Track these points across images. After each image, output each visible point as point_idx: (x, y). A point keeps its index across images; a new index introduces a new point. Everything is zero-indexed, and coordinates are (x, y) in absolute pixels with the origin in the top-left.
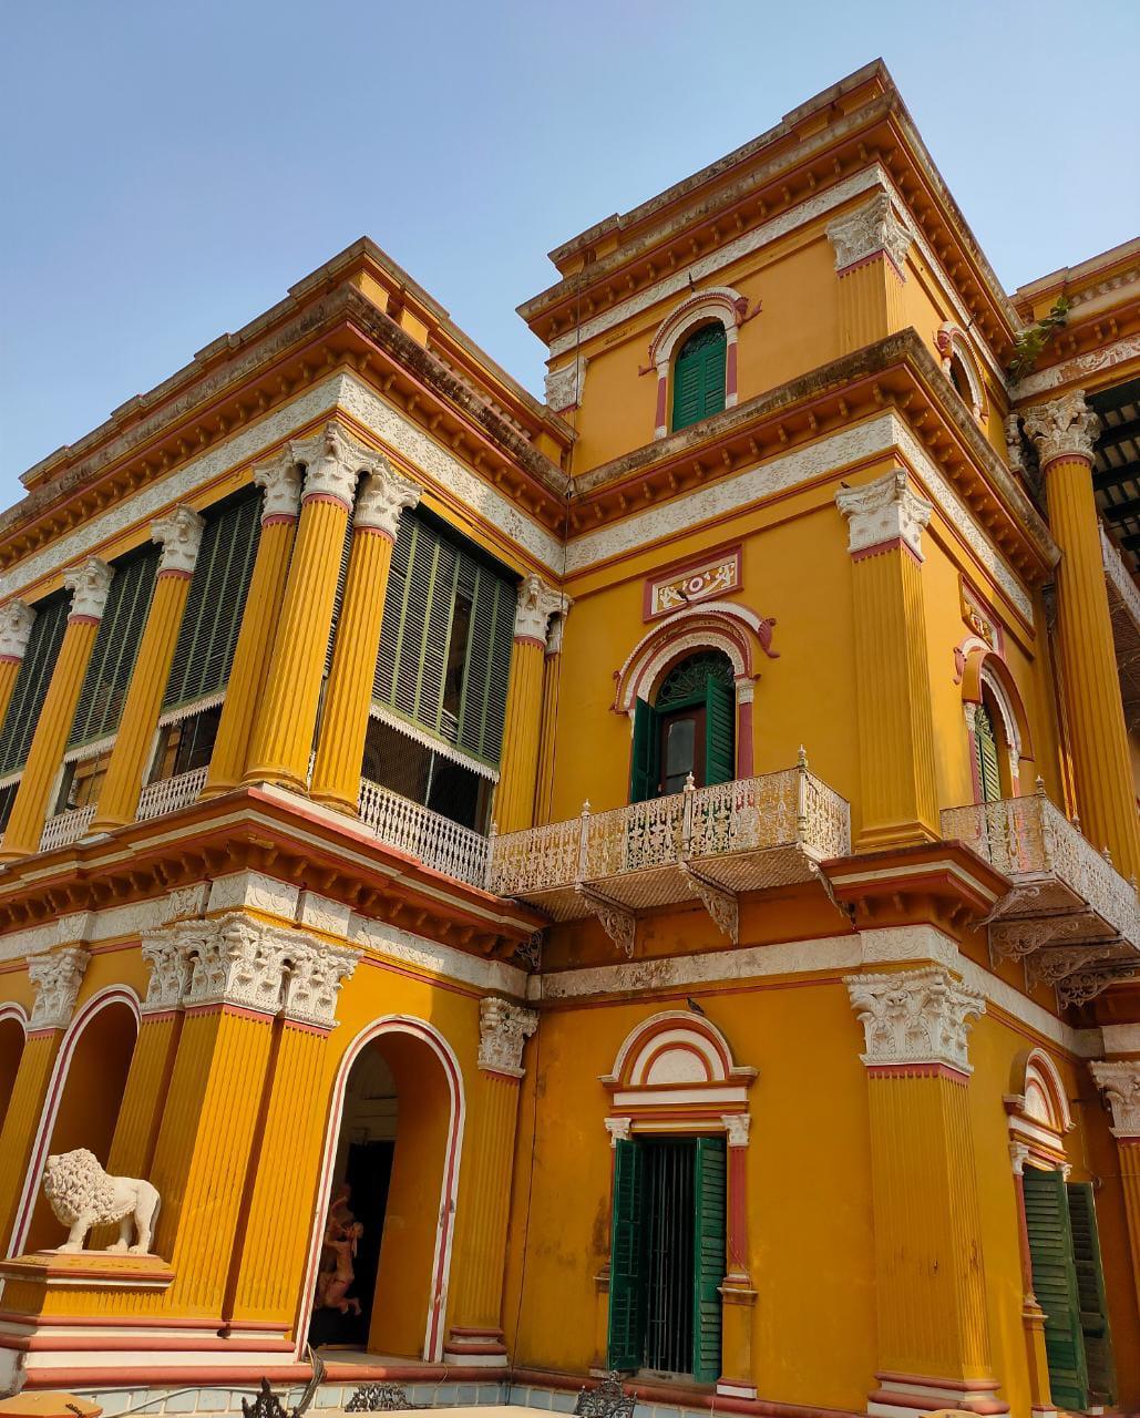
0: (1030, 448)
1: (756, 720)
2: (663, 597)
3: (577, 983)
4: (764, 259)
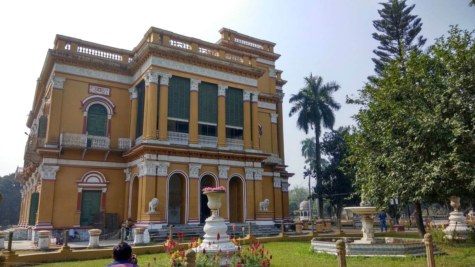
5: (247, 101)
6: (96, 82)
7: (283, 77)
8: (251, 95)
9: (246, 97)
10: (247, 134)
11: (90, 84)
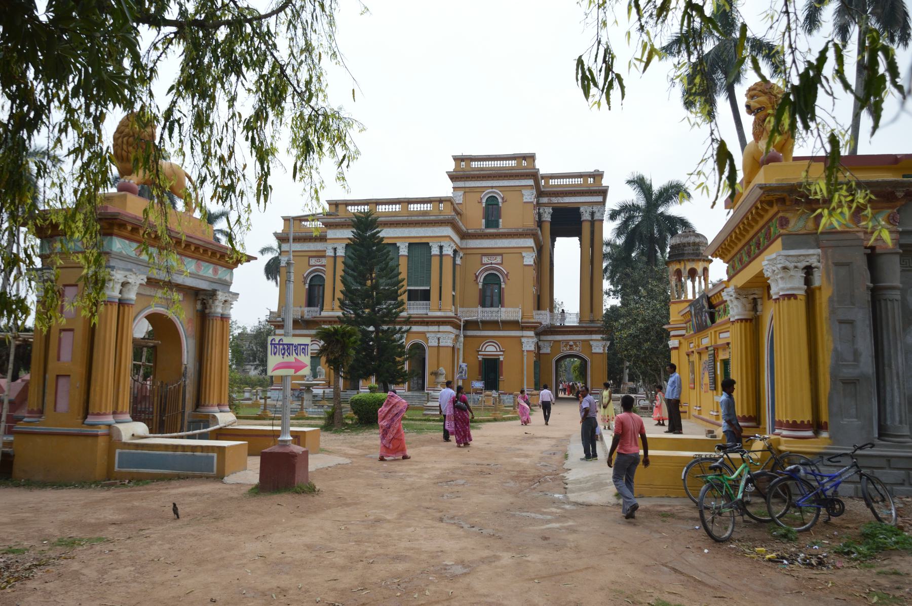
0: (540, 215)
1: (505, 291)
2: (485, 260)
3: (470, 333)
4: (508, 189)
5: (435, 255)
6: (314, 254)
7: (605, 182)
8: (441, 247)
9: (435, 251)
10: (434, 295)
11: (310, 257)
